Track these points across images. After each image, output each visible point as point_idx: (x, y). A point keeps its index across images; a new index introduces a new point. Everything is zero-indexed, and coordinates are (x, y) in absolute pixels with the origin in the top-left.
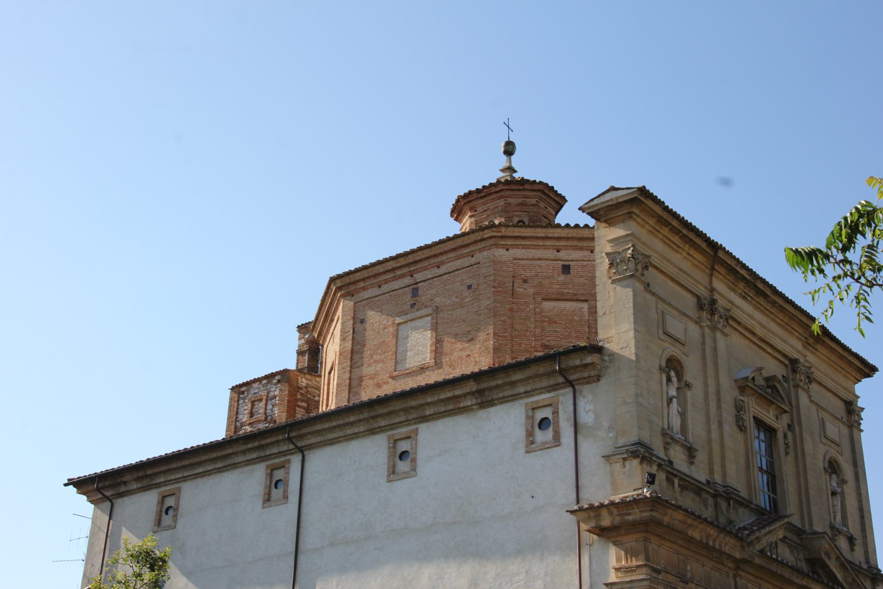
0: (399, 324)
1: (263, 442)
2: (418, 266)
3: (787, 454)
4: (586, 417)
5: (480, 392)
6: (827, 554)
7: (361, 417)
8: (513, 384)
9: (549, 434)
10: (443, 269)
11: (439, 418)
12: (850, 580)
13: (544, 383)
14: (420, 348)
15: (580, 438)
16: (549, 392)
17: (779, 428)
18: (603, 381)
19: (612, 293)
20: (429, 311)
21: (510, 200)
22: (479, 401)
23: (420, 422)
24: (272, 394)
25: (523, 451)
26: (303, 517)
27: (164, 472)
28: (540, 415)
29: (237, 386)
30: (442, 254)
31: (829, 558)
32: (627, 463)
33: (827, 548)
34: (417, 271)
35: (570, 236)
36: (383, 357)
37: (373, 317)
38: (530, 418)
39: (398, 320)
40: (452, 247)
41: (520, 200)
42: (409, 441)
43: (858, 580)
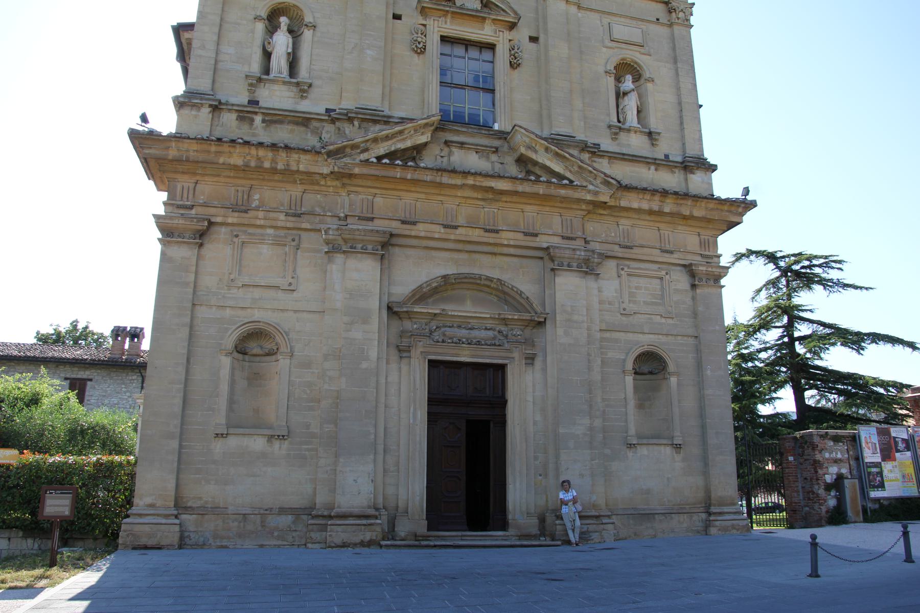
3: (514, 65)
6: (529, 147)
12: (576, 168)
17: (498, 41)
31: (536, 152)
33: (527, 141)
43: (585, 166)
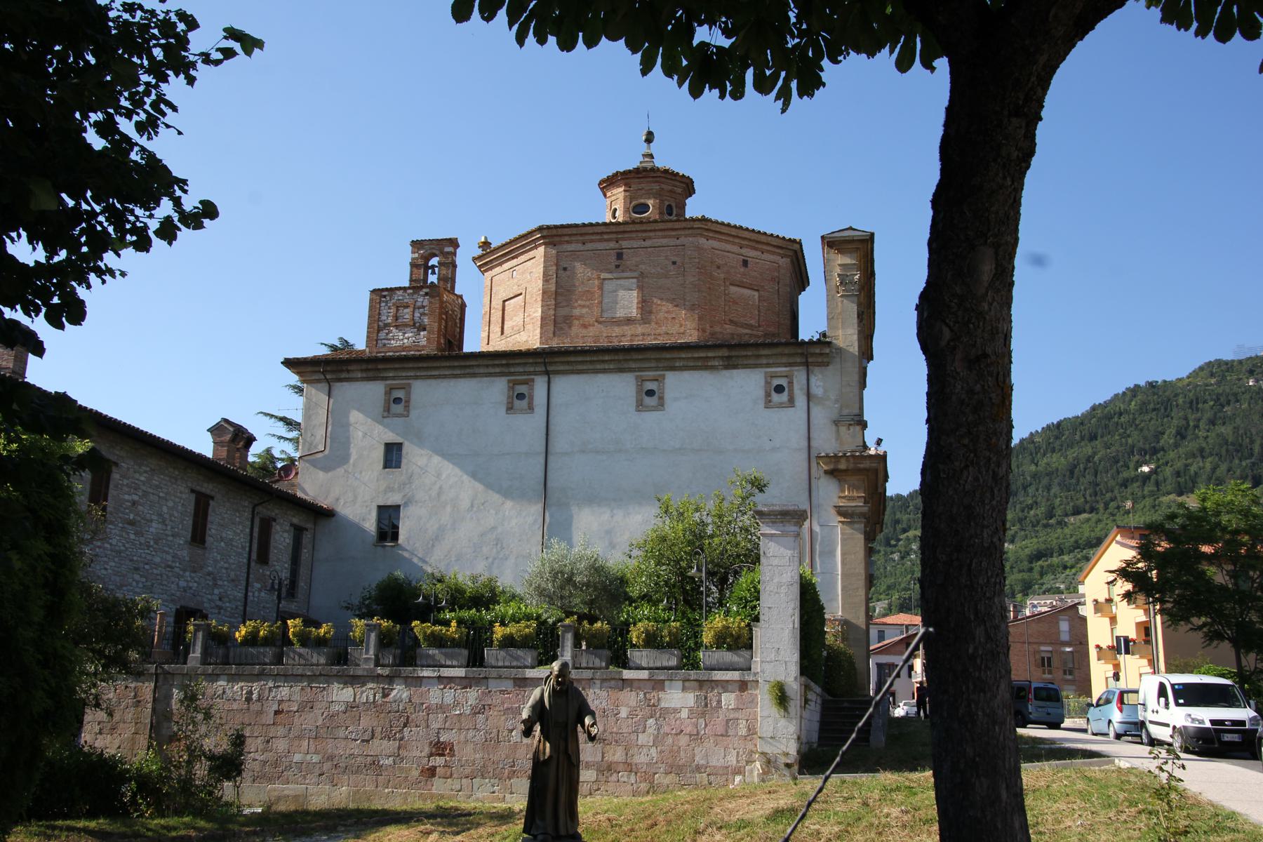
0: (604, 279)
1: (511, 362)
2: (626, 235)
4: (817, 390)
5: (729, 358)
7: (616, 358)
8: (758, 356)
9: (784, 397)
10: (648, 243)
11: (685, 370)
13: (784, 360)
14: (626, 303)
15: (811, 403)
16: (786, 367)
18: (831, 367)
19: (839, 304)
20: (635, 274)
21: (663, 186)
22: (726, 363)
23: (667, 370)
24: (419, 304)
25: (762, 405)
26: (551, 427)
27: (396, 369)
28: (776, 382)
29: (379, 289)
30: (651, 231)
32: (851, 428)
34: (624, 239)
35: (752, 238)
36: (588, 303)
37: (581, 271)
38: (767, 383)
39: (603, 275)
40: (663, 227)
41: (670, 188)
42: (656, 383)
